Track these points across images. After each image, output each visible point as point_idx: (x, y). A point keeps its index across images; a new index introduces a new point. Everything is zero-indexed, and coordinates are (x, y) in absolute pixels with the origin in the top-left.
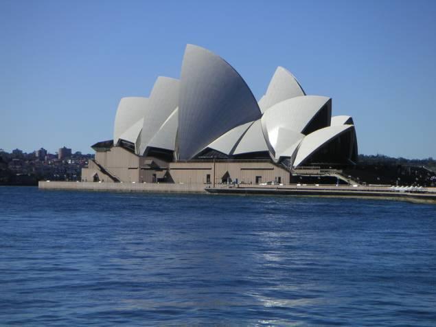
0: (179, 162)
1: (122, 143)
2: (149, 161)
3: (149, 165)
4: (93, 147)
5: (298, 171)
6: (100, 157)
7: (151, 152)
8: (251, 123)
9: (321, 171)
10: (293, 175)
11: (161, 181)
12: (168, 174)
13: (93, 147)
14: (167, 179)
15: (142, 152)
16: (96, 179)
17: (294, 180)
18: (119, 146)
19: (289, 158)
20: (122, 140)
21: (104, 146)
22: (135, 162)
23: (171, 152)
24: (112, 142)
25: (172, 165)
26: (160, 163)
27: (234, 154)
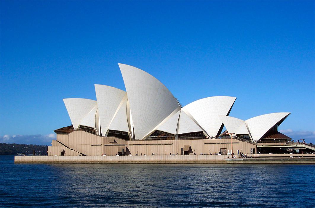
0: (135, 140)
1: (82, 128)
2: (112, 139)
4: (55, 131)
5: (262, 144)
6: (62, 137)
7: (112, 133)
8: (178, 113)
9: (286, 144)
11: (120, 153)
12: (127, 149)
13: (54, 131)
14: (127, 152)
15: (104, 134)
16: (63, 154)
18: (79, 130)
20: (81, 126)
21: (67, 130)
23: (127, 133)
24: (72, 126)
25: (129, 142)
26: (120, 141)
27: (180, 133)
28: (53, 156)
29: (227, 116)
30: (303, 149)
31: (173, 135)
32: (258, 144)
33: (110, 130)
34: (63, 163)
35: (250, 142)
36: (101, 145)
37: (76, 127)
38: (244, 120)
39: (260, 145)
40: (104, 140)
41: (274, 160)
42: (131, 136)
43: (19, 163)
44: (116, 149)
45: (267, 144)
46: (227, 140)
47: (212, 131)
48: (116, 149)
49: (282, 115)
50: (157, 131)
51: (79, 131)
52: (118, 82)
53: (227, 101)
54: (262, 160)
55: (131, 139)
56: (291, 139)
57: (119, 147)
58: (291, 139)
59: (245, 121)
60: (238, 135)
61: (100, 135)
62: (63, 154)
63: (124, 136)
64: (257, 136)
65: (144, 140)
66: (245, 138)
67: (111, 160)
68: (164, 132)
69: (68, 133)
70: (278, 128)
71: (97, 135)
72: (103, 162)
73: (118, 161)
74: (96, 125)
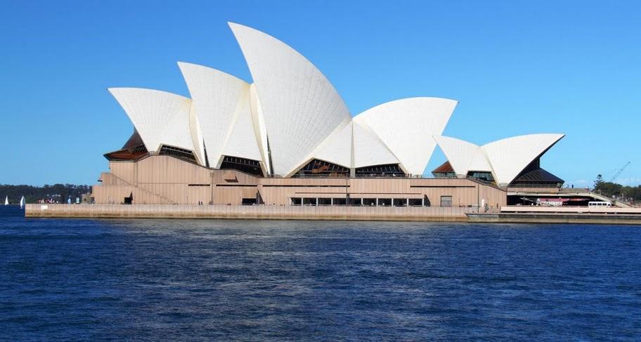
1: (167, 151)
2: (230, 174)
3: (226, 180)
5: (517, 189)
6: (125, 167)
7: (229, 163)
8: (348, 127)
10: (509, 194)
11: (247, 202)
12: (259, 195)
15: (215, 162)
16: (128, 201)
17: (512, 200)
19: (490, 173)
20: (164, 146)
22: (205, 177)
23: (257, 162)
25: (263, 181)
26: (243, 178)
28: (105, 204)
29: (442, 135)
30: (581, 200)
31: (346, 169)
32: (509, 189)
33: (226, 157)
34: (127, 220)
35: (495, 187)
36: (209, 185)
37: (152, 145)
38: (480, 145)
39: (515, 192)
40: (212, 175)
41: (552, 218)
42: (267, 169)
43: (36, 219)
44: (239, 194)
45: (525, 189)
46: (453, 182)
47: (416, 164)
48: (239, 194)
49: (550, 138)
50: (315, 160)
51: (161, 156)
52: (235, 64)
53: (443, 108)
54: (531, 217)
55: (265, 175)
56: (562, 182)
57: (241, 192)
58: (562, 182)
59: (482, 147)
60: (470, 173)
61: (205, 165)
62: (128, 201)
63: (252, 168)
64: (505, 176)
65: (292, 177)
66: (485, 178)
67: (244, 213)
68: (327, 163)
69: (136, 160)
70: (541, 158)
71: (201, 166)
72: (228, 217)
73: (258, 216)
74: (196, 145)
